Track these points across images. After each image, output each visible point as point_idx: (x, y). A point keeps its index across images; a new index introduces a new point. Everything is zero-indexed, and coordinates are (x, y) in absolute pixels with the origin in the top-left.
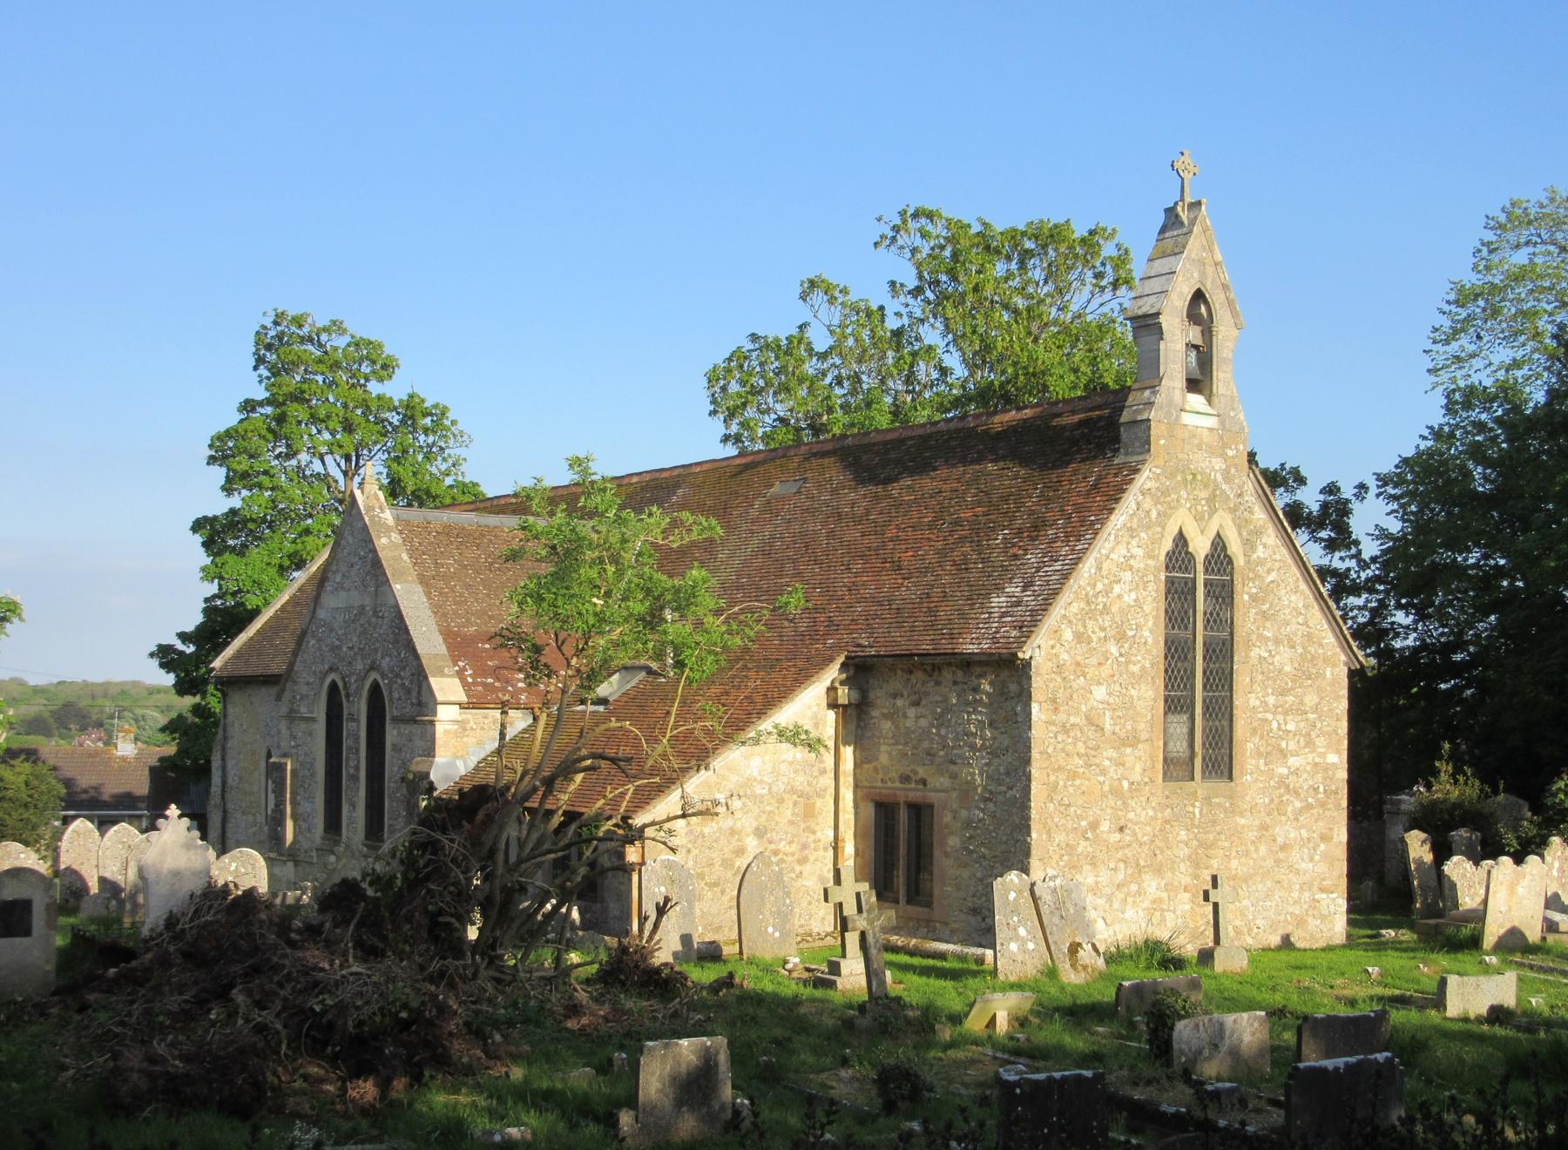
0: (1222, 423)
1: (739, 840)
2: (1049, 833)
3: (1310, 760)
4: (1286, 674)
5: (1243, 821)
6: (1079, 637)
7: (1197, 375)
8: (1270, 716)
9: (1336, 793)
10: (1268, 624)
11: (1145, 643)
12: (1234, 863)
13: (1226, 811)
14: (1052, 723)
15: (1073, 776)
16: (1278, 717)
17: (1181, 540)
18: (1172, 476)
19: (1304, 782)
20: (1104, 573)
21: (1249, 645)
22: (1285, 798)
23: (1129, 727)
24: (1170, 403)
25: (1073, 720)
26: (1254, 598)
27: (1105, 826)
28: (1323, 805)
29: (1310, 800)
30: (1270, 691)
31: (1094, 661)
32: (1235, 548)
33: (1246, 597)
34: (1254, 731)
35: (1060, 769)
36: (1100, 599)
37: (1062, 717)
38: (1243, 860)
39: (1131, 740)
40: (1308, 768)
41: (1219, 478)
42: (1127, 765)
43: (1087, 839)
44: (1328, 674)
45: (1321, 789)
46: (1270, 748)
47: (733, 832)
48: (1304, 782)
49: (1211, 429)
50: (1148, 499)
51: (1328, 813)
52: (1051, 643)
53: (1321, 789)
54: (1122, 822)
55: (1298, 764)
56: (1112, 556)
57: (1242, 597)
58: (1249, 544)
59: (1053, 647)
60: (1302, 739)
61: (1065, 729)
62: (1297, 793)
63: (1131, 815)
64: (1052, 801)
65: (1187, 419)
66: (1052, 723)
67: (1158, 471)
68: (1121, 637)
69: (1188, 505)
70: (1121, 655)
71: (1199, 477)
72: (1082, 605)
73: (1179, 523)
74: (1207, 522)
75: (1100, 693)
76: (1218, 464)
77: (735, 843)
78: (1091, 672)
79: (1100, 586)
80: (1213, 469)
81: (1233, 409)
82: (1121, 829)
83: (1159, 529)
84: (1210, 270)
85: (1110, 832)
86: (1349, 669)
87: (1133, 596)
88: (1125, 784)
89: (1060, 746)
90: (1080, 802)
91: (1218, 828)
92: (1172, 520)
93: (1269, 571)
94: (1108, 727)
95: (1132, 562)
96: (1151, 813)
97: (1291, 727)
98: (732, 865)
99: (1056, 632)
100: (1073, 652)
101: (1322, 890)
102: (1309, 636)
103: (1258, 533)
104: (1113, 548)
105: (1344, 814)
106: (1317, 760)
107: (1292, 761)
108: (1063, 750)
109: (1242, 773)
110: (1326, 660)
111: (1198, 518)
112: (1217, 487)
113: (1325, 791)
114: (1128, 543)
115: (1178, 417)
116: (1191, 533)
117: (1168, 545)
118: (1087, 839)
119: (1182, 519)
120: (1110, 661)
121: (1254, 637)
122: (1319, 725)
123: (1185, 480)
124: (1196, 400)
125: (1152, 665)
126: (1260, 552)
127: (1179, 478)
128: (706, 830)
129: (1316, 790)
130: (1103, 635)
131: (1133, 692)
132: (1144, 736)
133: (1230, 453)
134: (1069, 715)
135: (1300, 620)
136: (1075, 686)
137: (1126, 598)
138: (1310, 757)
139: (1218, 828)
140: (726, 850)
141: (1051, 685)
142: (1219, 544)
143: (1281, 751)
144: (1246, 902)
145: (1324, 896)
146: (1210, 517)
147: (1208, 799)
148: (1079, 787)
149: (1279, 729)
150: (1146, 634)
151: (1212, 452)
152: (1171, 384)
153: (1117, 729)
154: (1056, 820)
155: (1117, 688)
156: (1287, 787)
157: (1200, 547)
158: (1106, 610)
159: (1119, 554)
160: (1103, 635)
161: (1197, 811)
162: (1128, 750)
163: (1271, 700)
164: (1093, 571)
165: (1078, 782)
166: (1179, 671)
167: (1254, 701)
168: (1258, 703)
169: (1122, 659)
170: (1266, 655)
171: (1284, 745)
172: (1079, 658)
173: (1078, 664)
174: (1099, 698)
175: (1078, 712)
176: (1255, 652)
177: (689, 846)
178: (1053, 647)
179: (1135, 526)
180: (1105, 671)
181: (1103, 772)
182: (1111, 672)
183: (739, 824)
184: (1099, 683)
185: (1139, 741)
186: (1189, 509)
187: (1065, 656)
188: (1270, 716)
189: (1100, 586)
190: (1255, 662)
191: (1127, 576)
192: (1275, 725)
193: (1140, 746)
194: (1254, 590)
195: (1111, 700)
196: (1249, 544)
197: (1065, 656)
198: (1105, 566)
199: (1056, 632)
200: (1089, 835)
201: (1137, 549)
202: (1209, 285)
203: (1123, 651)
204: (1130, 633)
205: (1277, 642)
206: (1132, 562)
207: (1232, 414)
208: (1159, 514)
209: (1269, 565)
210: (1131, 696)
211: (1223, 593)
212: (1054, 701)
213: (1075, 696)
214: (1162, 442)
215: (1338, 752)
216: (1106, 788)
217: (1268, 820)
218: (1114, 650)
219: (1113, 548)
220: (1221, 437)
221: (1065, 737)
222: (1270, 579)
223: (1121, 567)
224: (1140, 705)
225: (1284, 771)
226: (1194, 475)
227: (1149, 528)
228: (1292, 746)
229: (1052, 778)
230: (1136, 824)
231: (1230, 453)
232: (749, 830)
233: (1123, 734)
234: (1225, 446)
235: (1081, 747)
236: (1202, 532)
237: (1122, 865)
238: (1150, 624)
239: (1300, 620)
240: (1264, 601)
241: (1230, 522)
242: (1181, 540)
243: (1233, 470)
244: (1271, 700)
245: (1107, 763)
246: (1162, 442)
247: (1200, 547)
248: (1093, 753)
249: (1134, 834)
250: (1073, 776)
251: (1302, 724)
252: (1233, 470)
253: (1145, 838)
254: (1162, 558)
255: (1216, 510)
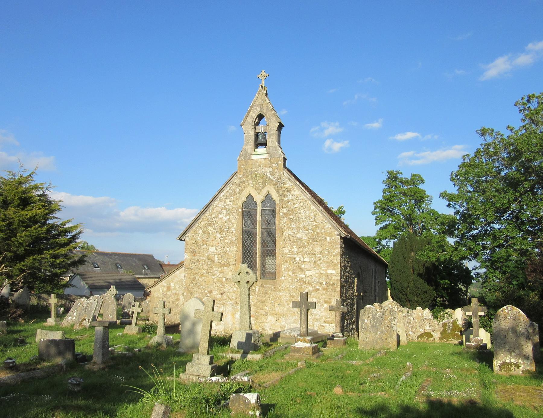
0: (271, 156)
1: (178, 296)
2: (191, 293)
3: (318, 272)
4: (304, 240)
5: (281, 293)
6: (204, 232)
7: (263, 141)
8: (295, 256)
9: (333, 284)
10: (293, 223)
11: (232, 233)
12: (277, 309)
13: (272, 290)
14: (193, 259)
15: (202, 276)
16: (299, 256)
17: (250, 197)
18: (247, 177)
19: (315, 280)
20: (215, 211)
21: (282, 230)
22: (303, 286)
23: (225, 260)
24: (246, 154)
25: (202, 258)
26: (285, 214)
27: (215, 293)
28: (325, 289)
29: (318, 287)
30: (295, 247)
31: (210, 239)
32: (275, 196)
33: (281, 214)
34: (286, 261)
35: (196, 274)
36: (214, 220)
37: (197, 257)
38: (281, 308)
39: (228, 264)
40: (317, 275)
41: (269, 174)
42: (225, 273)
43: (207, 296)
44: (328, 239)
45: (324, 283)
46: (294, 268)
47: (176, 294)
48: (315, 280)
49: (265, 159)
50: (234, 186)
51: (328, 293)
52: (193, 234)
53: (324, 283)
54: (222, 292)
55: (311, 274)
56: (218, 206)
57: (280, 214)
58: (282, 196)
59: (193, 236)
60: (312, 265)
61: (198, 261)
62: (310, 284)
63: (226, 289)
64: (192, 283)
65: (253, 157)
66: (193, 259)
67: (241, 176)
68: (221, 232)
69: (252, 185)
70: (222, 237)
71: (258, 175)
72: (206, 222)
73: (248, 191)
74: (261, 190)
75: (212, 250)
76: (269, 170)
77: (176, 297)
78: (209, 243)
79: (214, 216)
80: (266, 172)
81: (276, 150)
82: (222, 294)
83: (239, 195)
84: (265, 107)
85: (217, 294)
86: (341, 237)
87: (228, 217)
88: (224, 279)
89: (196, 267)
90: (204, 284)
91: (268, 296)
92: (244, 191)
93: (294, 204)
94: (216, 260)
95: (227, 207)
96: (235, 289)
97: (306, 259)
98: (175, 303)
99: (195, 231)
100: (201, 237)
101: (325, 322)
102: (316, 226)
103: (288, 191)
104: (218, 203)
105: (339, 293)
106: (322, 272)
107: (307, 272)
108: (197, 268)
109: (279, 277)
110: (327, 235)
111: (257, 189)
112: (267, 178)
113: (326, 284)
114: (225, 201)
115: (249, 158)
116: (254, 194)
117: (243, 199)
118: (207, 296)
119: (250, 190)
120: (217, 239)
121: (285, 228)
122: (322, 259)
123: (252, 177)
124: (261, 150)
125: (236, 240)
126: (290, 197)
127: (249, 177)
128: (168, 293)
129: (321, 283)
130: (214, 231)
131: (228, 249)
132: (231, 263)
133: (274, 165)
134: (200, 257)
135: (312, 220)
136: (202, 247)
137: (224, 218)
138: (317, 271)
139: (268, 296)
140: (174, 299)
141: (193, 248)
142: (268, 197)
143: (301, 269)
144: (283, 323)
145: (327, 325)
146: (263, 188)
147: (262, 286)
148: (204, 280)
149: (300, 260)
150: (233, 229)
151: (265, 166)
152: (246, 147)
153: (220, 261)
154: (194, 290)
155: (220, 248)
156: (305, 282)
157: (259, 198)
158: (216, 223)
159: (221, 205)
160: (214, 231)
161: (257, 289)
162: (225, 268)
163: (296, 250)
164: (211, 211)
165: (203, 278)
166: (252, 241)
167: (286, 250)
168: (288, 251)
169: (223, 238)
170: (292, 234)
171: (303, 266)
172: (204, 239)
173: (204, 241)
174: (212, 251)
175: (204, 255)
176: (285, 234)
177: (163, 297)
178: (193, 236)
179: (228, 195)
180: (215, 242)
181: (214, 275)
182: (217, 243)
183: (177, 292)
184: (212, 246)
185: (230, 265)
186: (253, 186)
187: (199, 238)
188: (295, 256)
189: (214, 216)
190: (286, 236)
191: (225, 211)
192: (298, 259)
193: (230, 267)
194: (286, 211)
195: (217, 252)
196: (282, 196)
197: (199, 238)
198: (215, 209)
199: (195, 231)
200: (208, 295)
201: (229, 203)
202: (265, 111)
203: (223, 236)
204: (225, 230)
205: (298, 229)
206: (227, 207)
207: (275, 152)
208: (240, 190)
209: (294, 201)
210: (227, 251)
211: (273, 213)
212: (193, 252)
213: (202, 251)
214: (242, 166)
215: (334, 269)
216: (215, 280)
217: (294, 294)
218: (219, 236)
219: (218, 203)
220: (270, 161)
221: (198, 264)
222: (295, 207)
223: (222, 209)
224: (230, 253)
225: (304, 276)
226: (256, 175)
227: (234, 195)
228: (307, 266)
229: (192, 276)
230: (228, 292)
231: (274, 165)
232: (181, 294)
233: (223, 263)
234: (271, 163)
235: (205, 267)
236: (259, 194)
237: (223, 306)
238: (235, 226)
239: (312, 220)
240: (290, 214)
241: (273, 189)
242: (250, 197)
243: (276, 171)
244: (296, 250)
245: (216, 272)
246: (242, 166)
247: (259, 198)
248: (209, 269)
249: (228, 295)
250: (202, 276)
251: (313, 259)
252: (276, 171)
253: (233, 297)
254: (240, 204)
255: (266, 185)
